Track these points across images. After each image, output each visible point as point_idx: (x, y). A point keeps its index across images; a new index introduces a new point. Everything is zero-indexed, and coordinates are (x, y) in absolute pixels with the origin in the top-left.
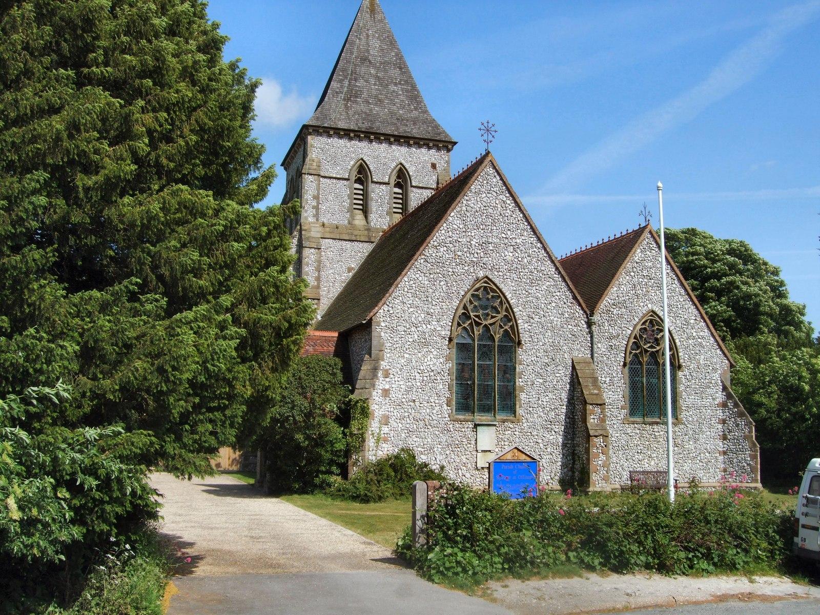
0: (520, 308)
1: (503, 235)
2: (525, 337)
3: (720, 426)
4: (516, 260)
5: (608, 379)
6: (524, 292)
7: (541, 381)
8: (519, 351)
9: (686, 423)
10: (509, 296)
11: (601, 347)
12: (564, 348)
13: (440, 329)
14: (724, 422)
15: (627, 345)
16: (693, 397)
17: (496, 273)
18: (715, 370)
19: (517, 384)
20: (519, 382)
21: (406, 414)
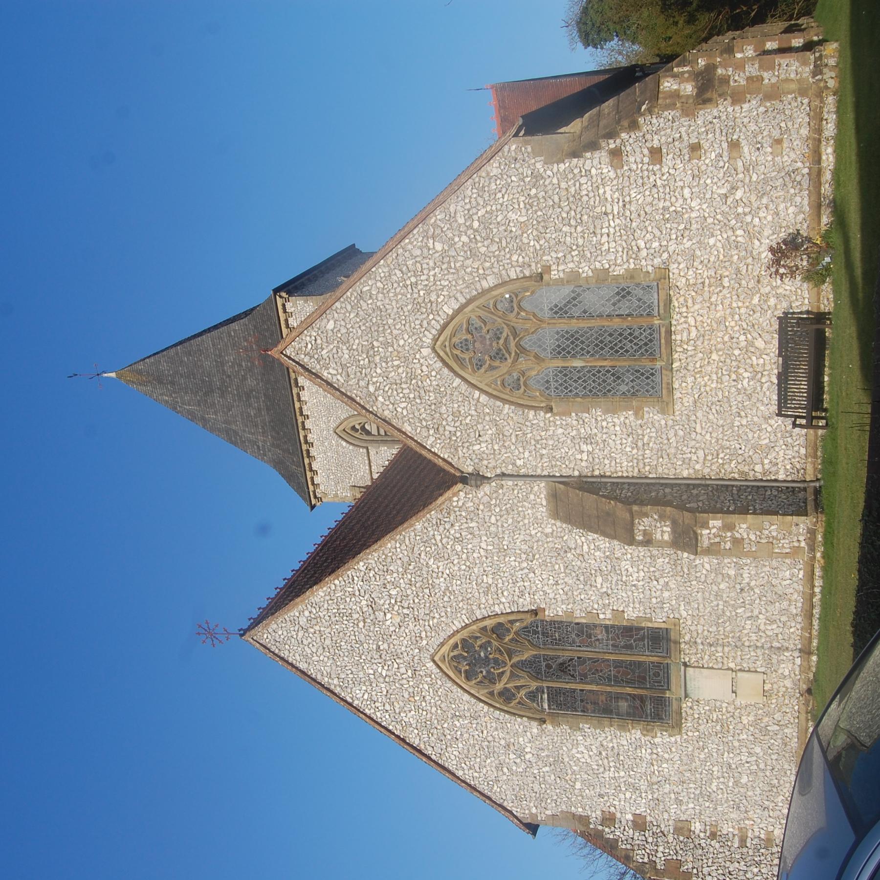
0: (474, 607)
1: (361, 624)
2: (525, 603)
3: (668, 160)
4: (396, 608)
5: (584, 447)
6: (446, 599)
7: (599, 580)
8: (549, 614)
9: (665, 255)
10: (458, 625)
11: (525, 461)
12: (533, 532)
13: (528, 734)
14: (656, 154)
15: (511, 403)
16: (605, 239)
17: (424, 642)
18: (537, 177)
19: (608, 622)
20: (606, 617)
21: (673, 796)
